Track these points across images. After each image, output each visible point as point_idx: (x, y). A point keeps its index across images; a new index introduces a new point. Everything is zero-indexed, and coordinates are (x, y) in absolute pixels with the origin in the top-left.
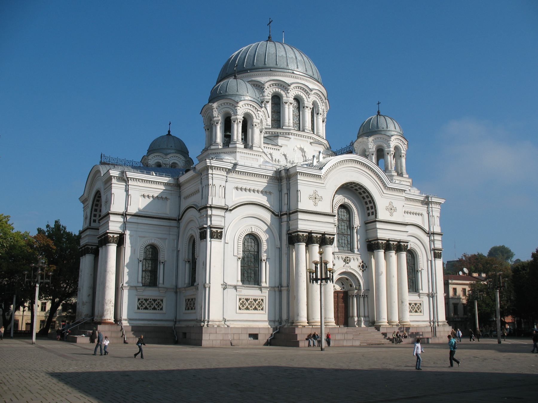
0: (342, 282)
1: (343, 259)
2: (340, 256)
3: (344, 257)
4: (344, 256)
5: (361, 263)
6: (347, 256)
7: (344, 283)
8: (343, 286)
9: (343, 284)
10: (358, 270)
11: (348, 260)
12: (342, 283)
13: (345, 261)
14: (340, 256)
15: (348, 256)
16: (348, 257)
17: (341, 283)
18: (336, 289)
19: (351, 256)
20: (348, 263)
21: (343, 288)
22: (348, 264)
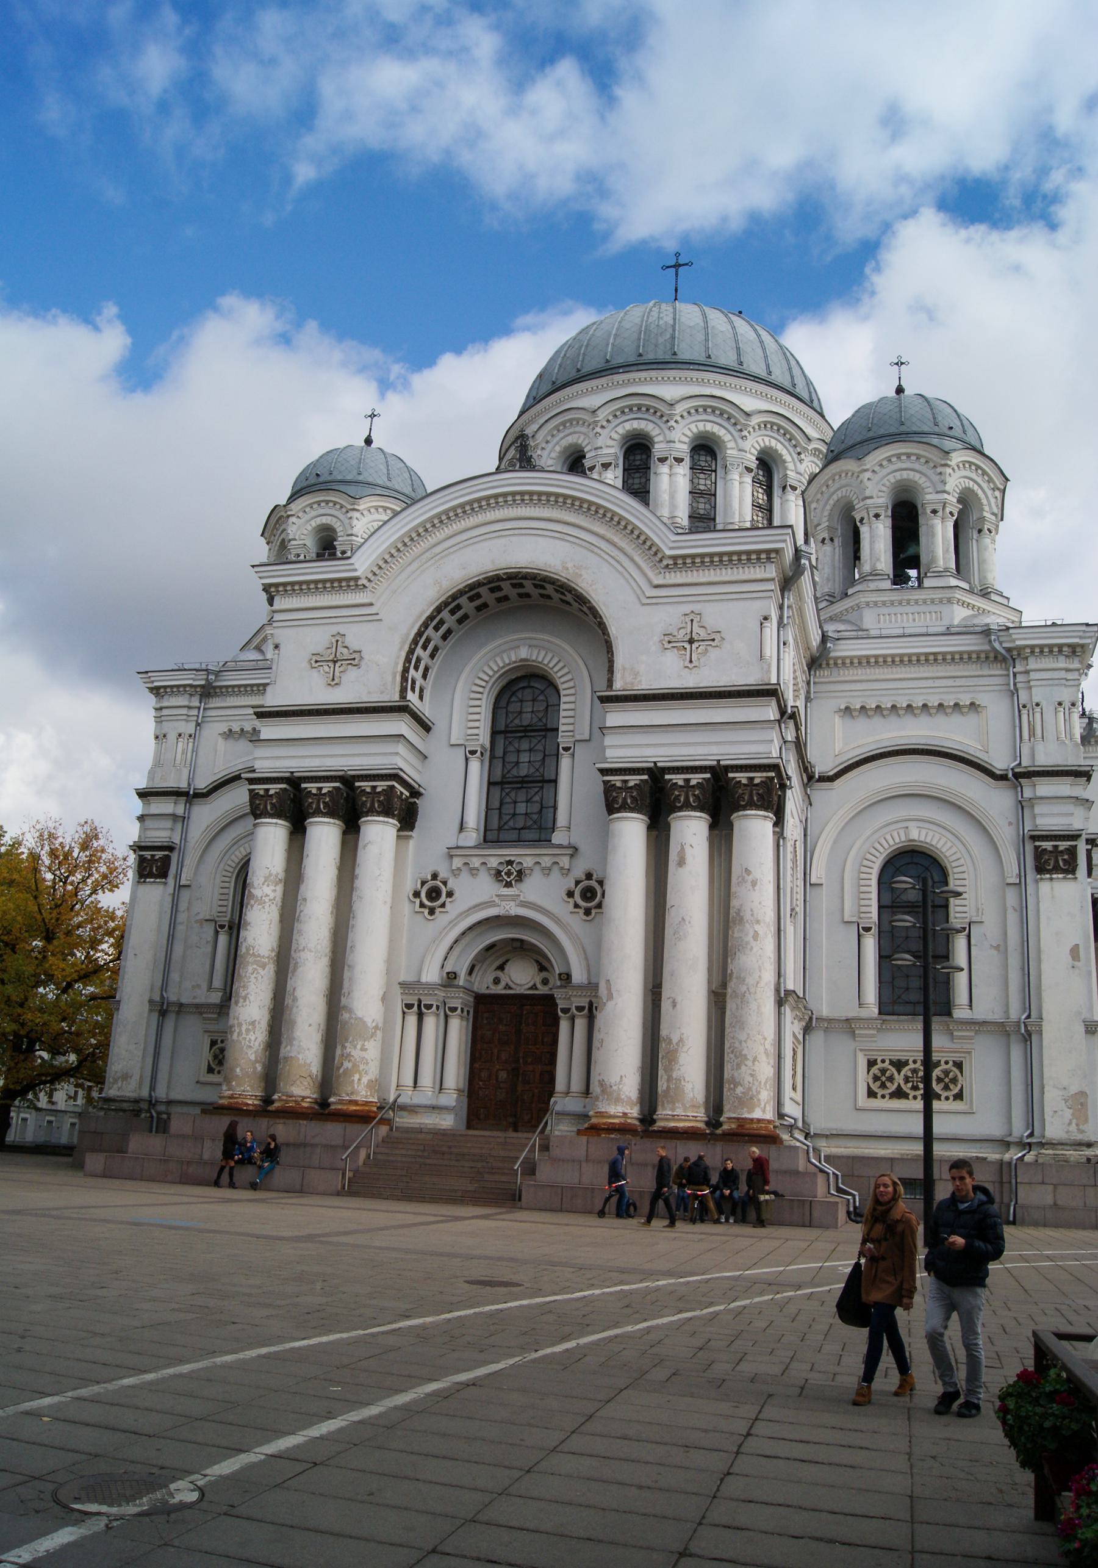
0: (541, 960)
1: (493, 872)
2: (476, 862)
3: (494, 863)
4: (495, 858)
5: (577, 883)
6: (508, 859)
7: (545, 964)
8: (544, 974)
9: (542, 968)
10: (562, 908)
11: (509, 874)
12: (537, 961)
13: (498, 873)
14: (476, 862)
15: (513, 859)
16: (510, 863)
17: (535, 965)
18: (510, 988)
19: (525, 856)
20: (508, 885)
21: (545, 982)
22: (510, 889)
